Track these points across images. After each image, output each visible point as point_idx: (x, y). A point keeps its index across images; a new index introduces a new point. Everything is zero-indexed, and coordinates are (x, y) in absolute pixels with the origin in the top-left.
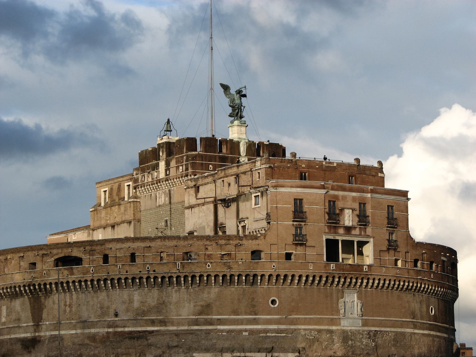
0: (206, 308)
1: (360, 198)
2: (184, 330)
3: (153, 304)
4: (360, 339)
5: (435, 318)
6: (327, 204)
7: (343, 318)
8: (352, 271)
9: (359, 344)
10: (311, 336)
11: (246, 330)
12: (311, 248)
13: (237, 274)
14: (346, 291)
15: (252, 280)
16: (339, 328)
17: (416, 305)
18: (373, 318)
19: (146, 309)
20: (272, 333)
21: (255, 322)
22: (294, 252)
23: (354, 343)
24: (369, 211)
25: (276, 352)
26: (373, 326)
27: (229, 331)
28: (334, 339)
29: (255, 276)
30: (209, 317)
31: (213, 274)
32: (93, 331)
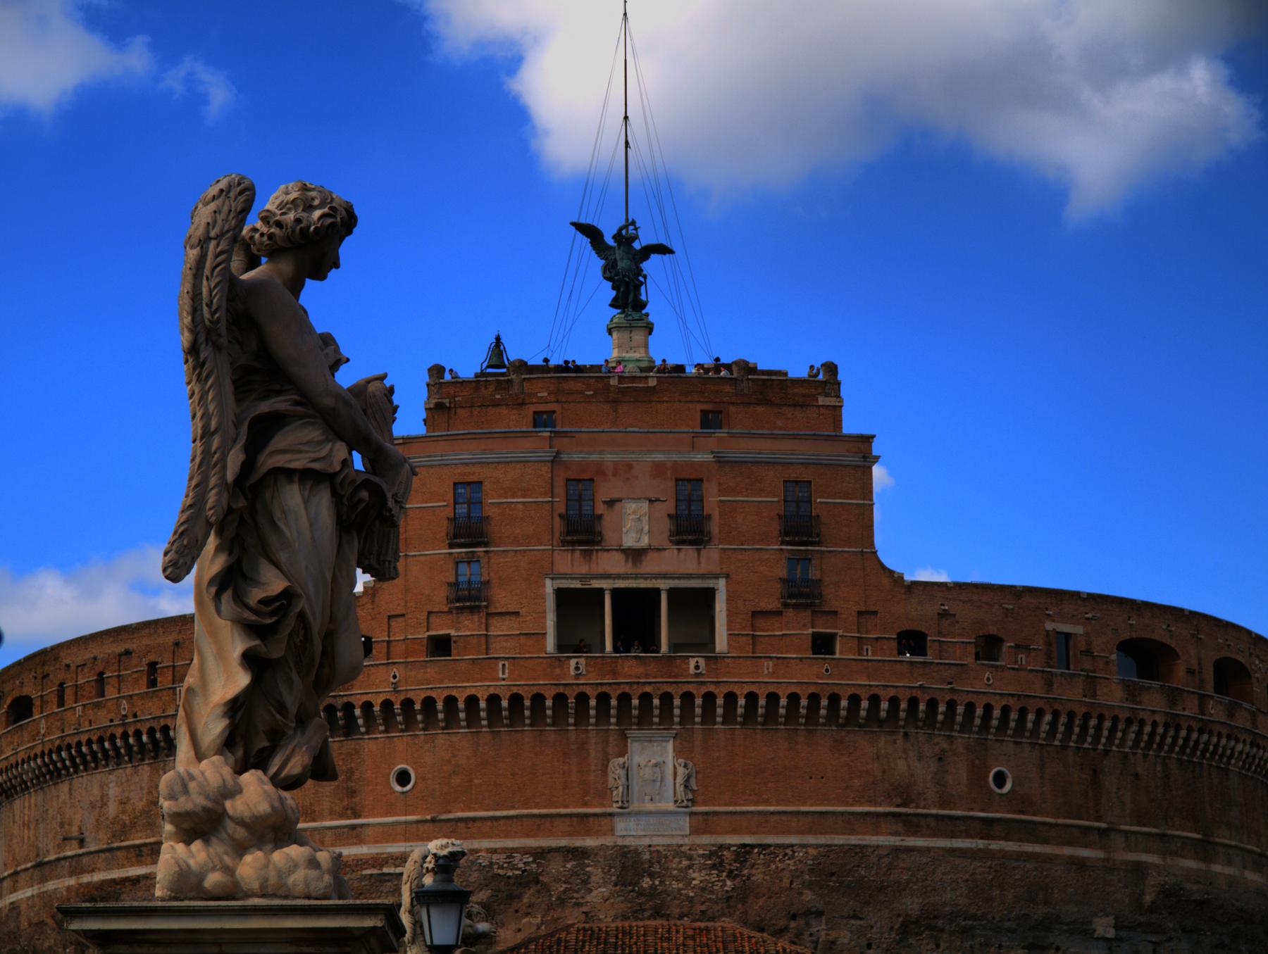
3: (140, 805)
4: (680, 870)
5: (1020, 801)
6: (560, 489)
7: (621, 814)
8: (647, 676)
9: (675, 885)
10: (514, 868)
12: (507, 618)
16: (608, 841)
18: (731, 809)
19: (125, 818)
21: (354, 834)
22: (453, 633)
24: (712, 499)
26: (735, 831)
28: (589, 875)
29: (349, 707)
32: (50, 886)
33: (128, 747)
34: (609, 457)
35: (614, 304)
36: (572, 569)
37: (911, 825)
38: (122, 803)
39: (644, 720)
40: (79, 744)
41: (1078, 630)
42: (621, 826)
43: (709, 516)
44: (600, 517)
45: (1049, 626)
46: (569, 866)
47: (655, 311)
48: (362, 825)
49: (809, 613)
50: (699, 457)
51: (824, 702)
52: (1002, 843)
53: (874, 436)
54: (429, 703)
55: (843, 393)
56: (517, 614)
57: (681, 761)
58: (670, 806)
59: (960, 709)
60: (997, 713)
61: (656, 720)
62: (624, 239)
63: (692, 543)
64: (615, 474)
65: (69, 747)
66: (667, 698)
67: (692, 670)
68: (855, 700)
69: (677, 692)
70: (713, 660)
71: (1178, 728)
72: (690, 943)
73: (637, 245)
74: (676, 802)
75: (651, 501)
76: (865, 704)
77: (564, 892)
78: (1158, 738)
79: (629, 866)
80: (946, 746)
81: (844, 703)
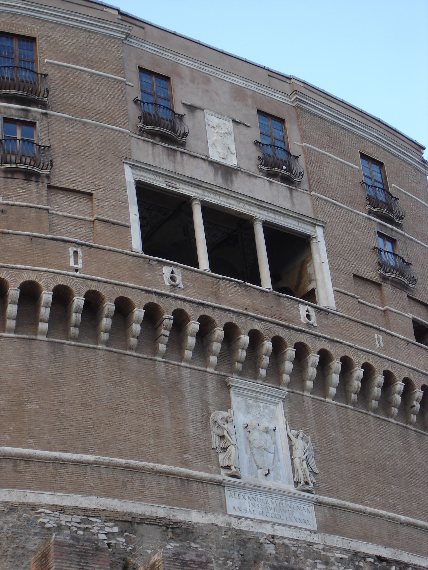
8: (255, 310)
12: (75, 198)
16: (220, 520)
26: (366, 538)
36: (156, 164)
42: (235, 502)
44: (181, 117)
49: (404, 295)
57: (293, 431)
58: (292, 488)
61: (263, 372)
64: (193, 81)
67: (303, 319)
69: (291, 339)
74: (297, 483)
75: (234, 121)
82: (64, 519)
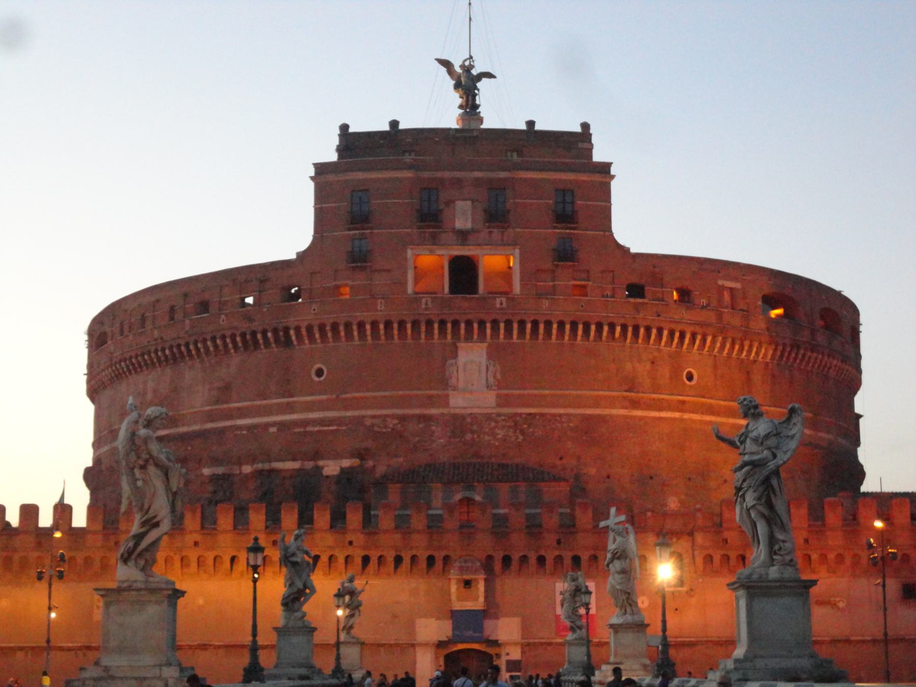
0: (225, 391)
1: (490, 180)
2: (194, 432)
9: (487, 438)
10: (386, 427)
11: (274, 424)
13: (260, 329)
14: (458, 344)
15: (283, 338)
16: (445, 411)
17: (637, 365)
20: (313, 426)
21: (289, 408)
23: (479, 436)
25: (322, 458)
27: (250, 428)
28: (433, 432)
29: (286, 330)
30: (225, 406)
31: (228, 333)
33: (158, 358)
34: (447, 174)
35: (461, 107)
37: (635, 404)
38: (155, 391)
39: (469, 337)
40: (131, 357)
41: (738, 285)
42: (452, 402)
43: (509, 211)
44: (441, 211)
45: (720, 282)
46: (421, 426)
47: (483, 111)
48: (294, 402)
50: (503, 175)
51: (581, 327)
52: (691, 415)
53: (611, 163)
54: (335, 327)
55: (593, 141)
56: (389, 271)
59: (665, 333)
60: (688, 336)
61: (475, 337)
62: (467, 69)
63: (498, 227)
65: (125, 360)
66: (482, 323)
67: (498, 306)
68: (599, 326)
70: (511, 299)
71: (798, 348)
72: (496, 473)
73: (474, 72)
75: (473, 202)
76: (606, 328)
77: (418, 442)
78: (786, 354)
79: (459, 425)
80: (656, 354)
81: (593, 327)
82: (376, 421)
